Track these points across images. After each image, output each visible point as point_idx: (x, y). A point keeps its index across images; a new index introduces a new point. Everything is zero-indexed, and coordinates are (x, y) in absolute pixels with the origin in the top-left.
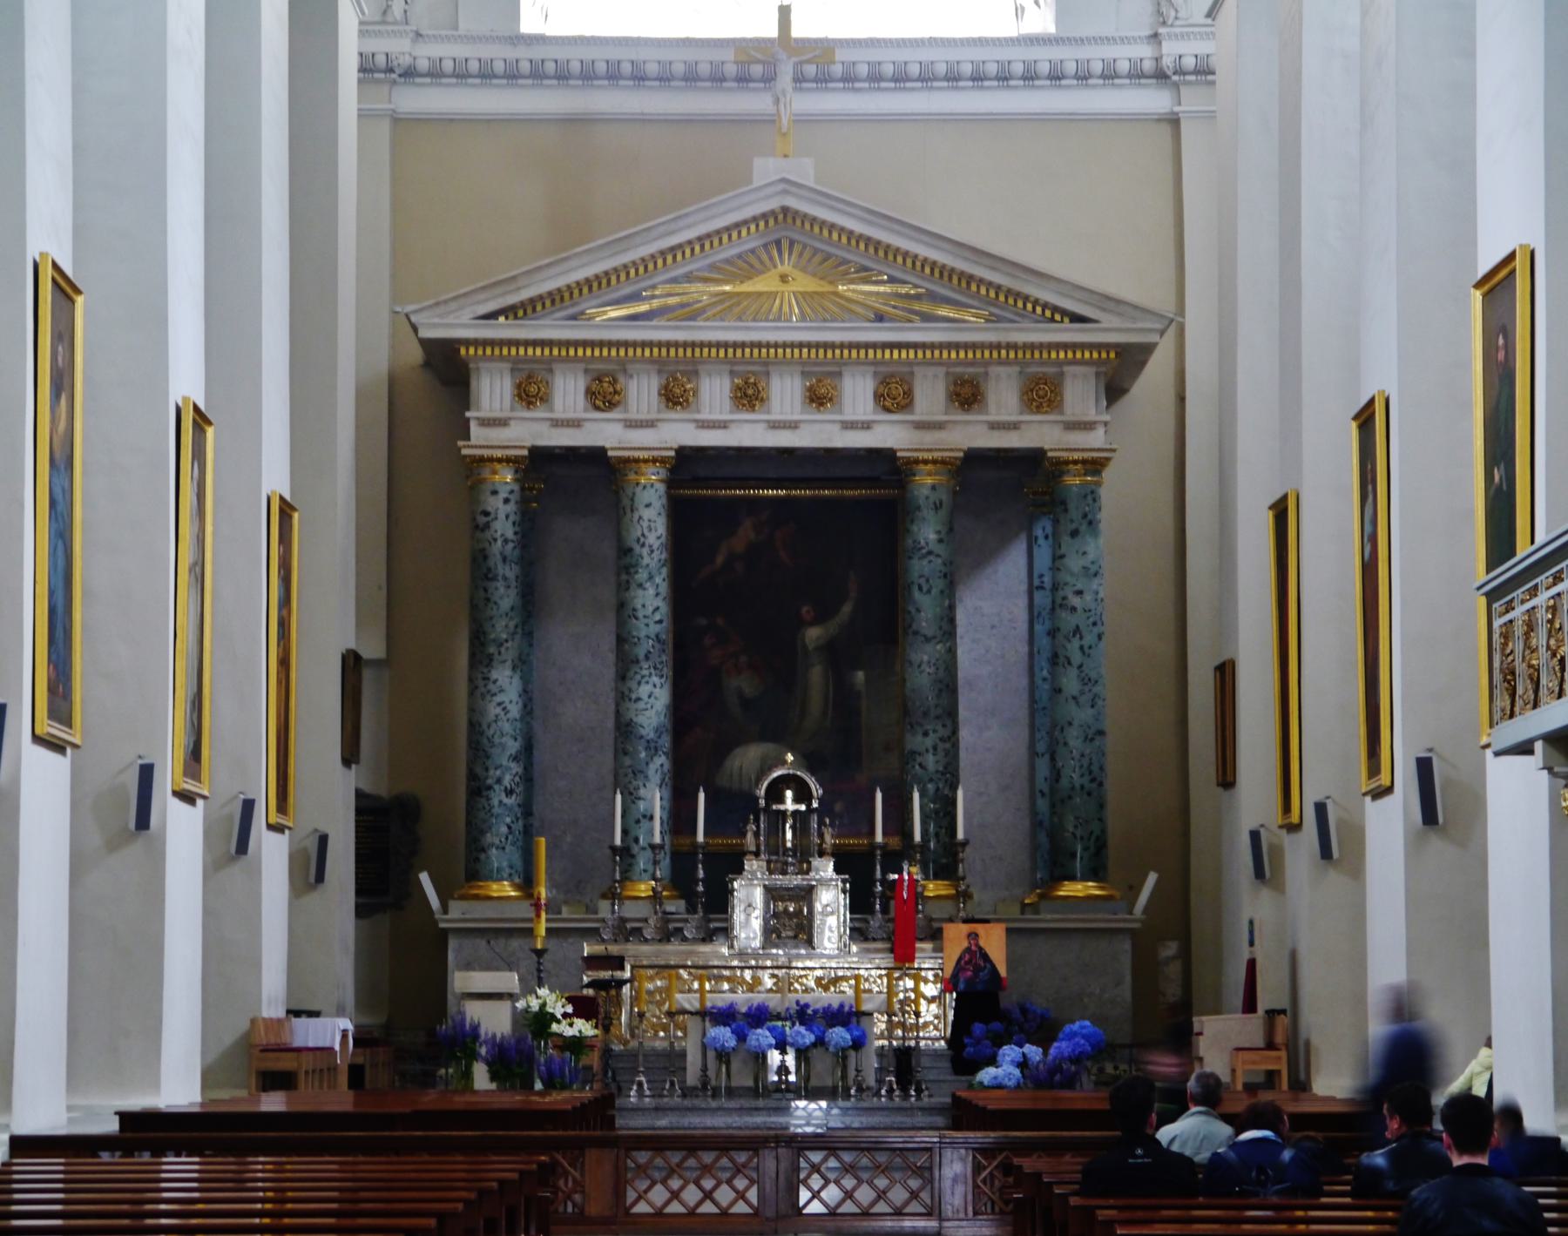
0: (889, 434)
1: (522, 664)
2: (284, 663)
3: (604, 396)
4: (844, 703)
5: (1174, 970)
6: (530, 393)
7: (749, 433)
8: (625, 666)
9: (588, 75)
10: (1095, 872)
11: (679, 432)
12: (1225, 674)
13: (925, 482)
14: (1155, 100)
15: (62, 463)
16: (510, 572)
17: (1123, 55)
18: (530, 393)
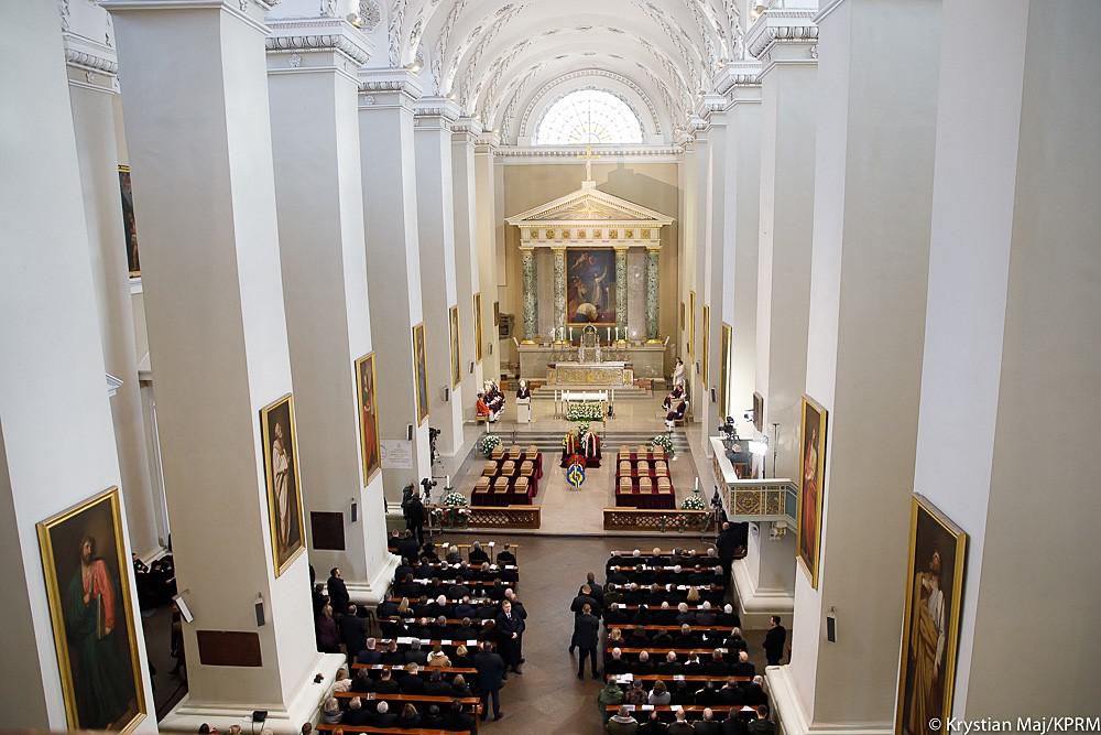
0: (612, 243)
1: (535, 295)
2: (479, 328)
3: (550, 235)
4: (604, 293)
5: (674, 350)
6: (534, 234)
7: (582, 243)
8: (556, 294)
9: (546, 155)
10: (656, 338)
11: (567, 243)
12: (683, 306)
13: (619, 254)
14: (672, 159)
15: (421, 366)
16: (531, 274)
17: (665, 149)
18: (534, 234)
